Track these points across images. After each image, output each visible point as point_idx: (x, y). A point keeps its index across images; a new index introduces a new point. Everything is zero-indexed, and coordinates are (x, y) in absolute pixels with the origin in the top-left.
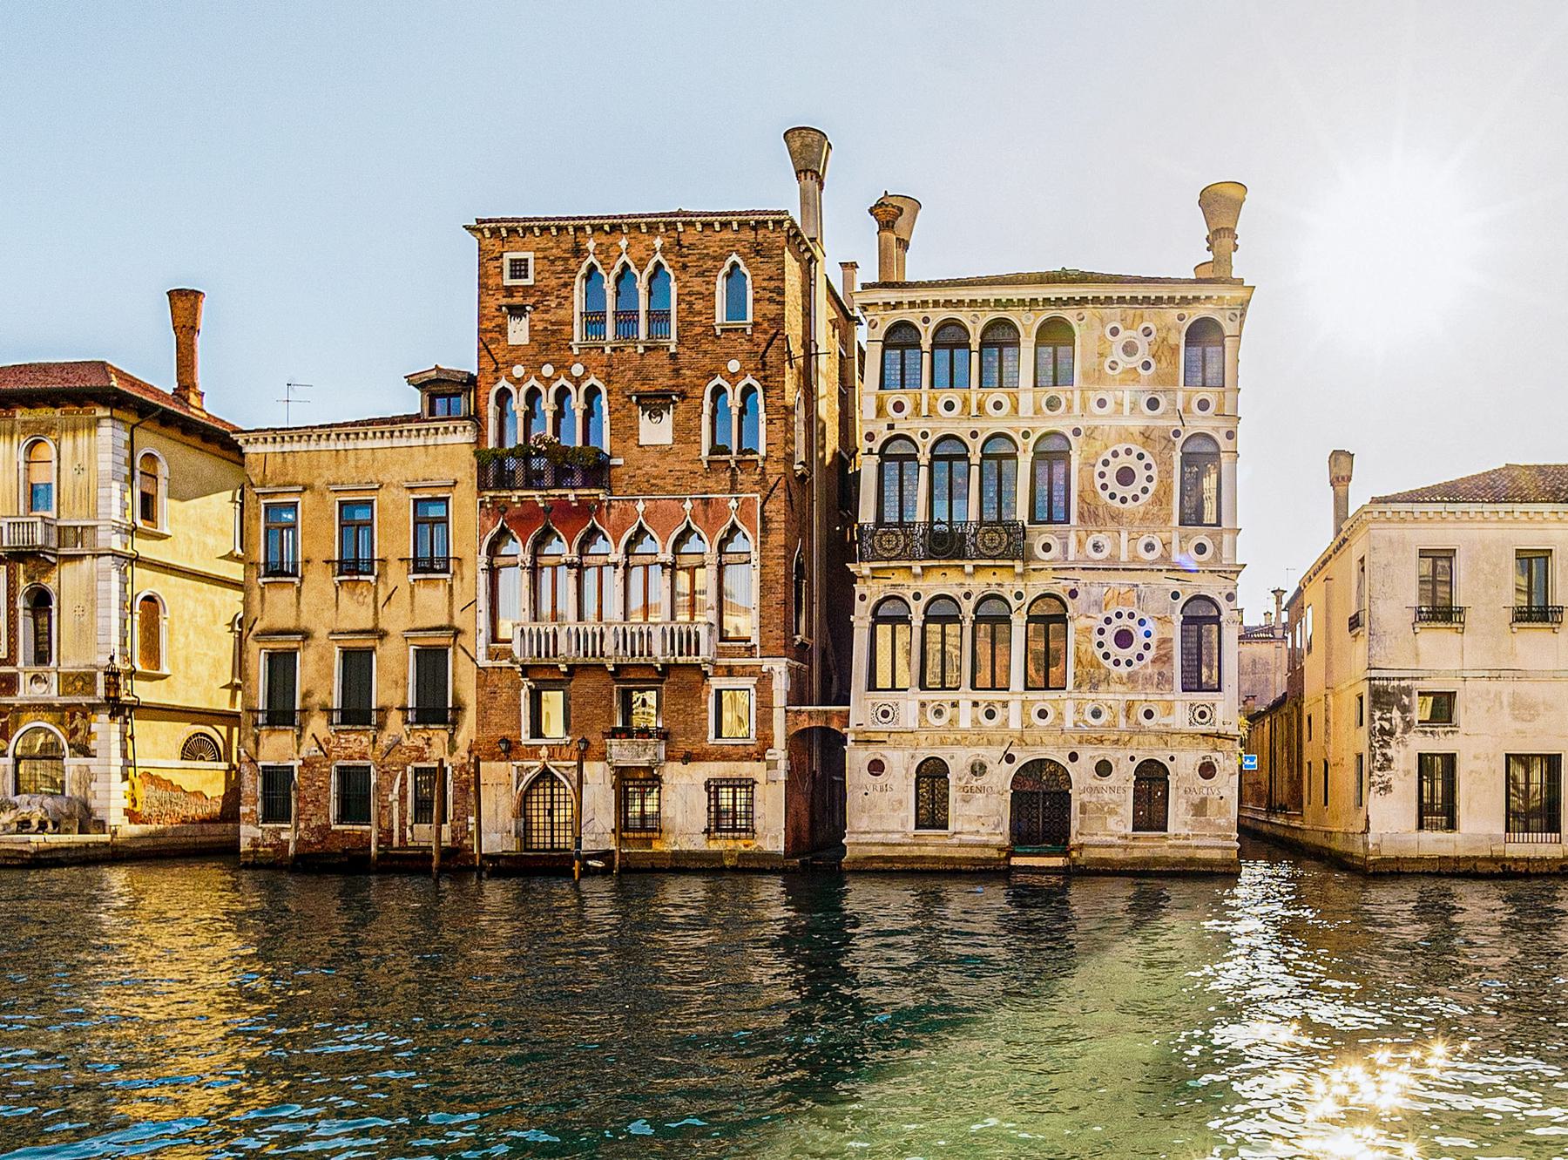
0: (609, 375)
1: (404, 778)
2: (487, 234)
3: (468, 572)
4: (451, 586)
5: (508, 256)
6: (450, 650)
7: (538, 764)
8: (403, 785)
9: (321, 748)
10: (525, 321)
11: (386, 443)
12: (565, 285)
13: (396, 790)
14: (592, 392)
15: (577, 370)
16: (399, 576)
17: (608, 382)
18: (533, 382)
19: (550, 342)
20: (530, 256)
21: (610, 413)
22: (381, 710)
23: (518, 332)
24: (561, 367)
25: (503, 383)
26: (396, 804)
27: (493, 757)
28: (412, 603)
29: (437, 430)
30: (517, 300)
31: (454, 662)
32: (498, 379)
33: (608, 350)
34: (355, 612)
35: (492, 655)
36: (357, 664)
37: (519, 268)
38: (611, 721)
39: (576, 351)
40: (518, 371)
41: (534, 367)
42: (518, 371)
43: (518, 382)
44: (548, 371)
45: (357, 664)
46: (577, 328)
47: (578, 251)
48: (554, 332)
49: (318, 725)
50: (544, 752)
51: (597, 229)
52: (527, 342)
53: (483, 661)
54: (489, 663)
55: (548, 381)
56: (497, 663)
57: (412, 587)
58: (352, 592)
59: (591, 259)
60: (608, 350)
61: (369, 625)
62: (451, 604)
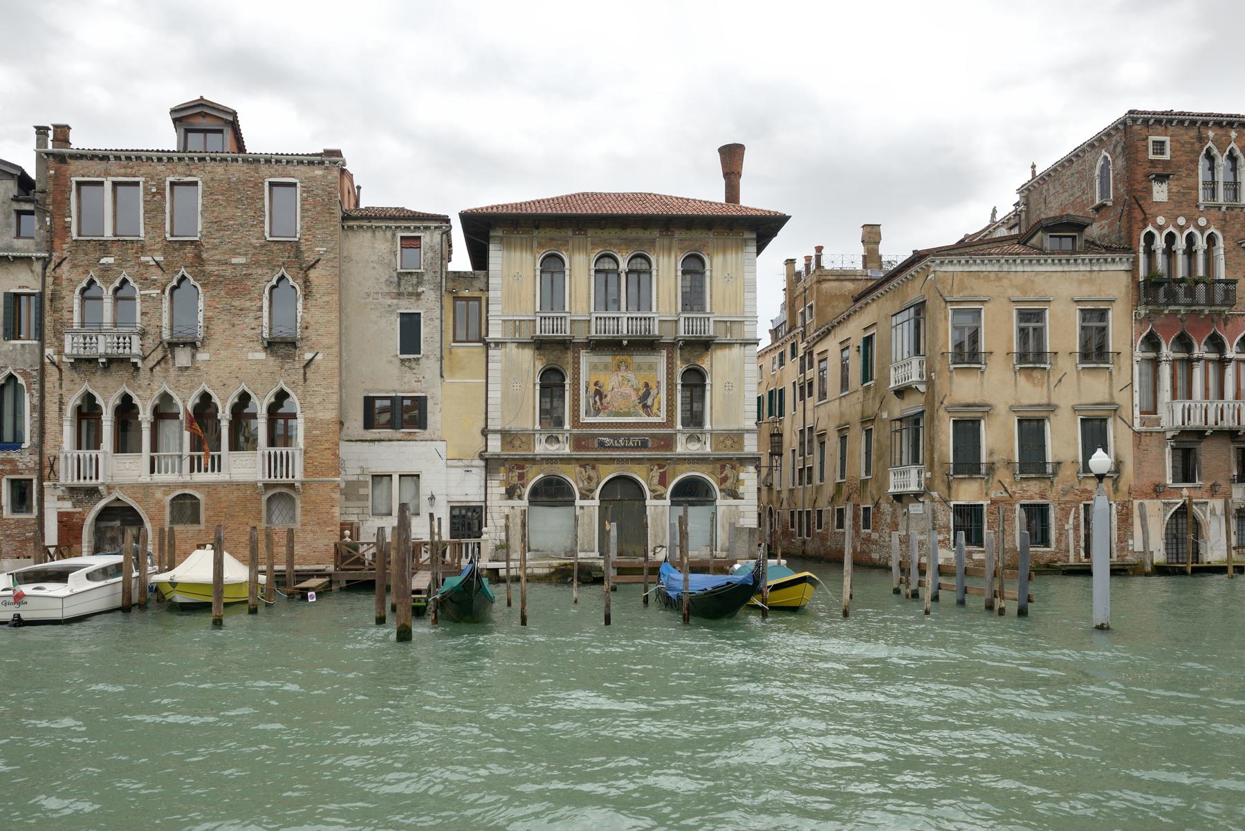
0: (1224, 226)
1: (1077, 512)
2: (1140, 122)
3: (1124, 362)
4: (1111, 373)
5: (1152, 138)
6: (1110, 421)
7: (1181, 501)
8: (1076, 518)
9: (1006, 491)
10: (1165, 186)
11: (1060, 269)
12: (1192, 162)
13: (1071, 521)
14: (1211, 240)
15: (1202, 222)
16: (1068, 365)
17: (1223, 232)
18: (1171, 229)
19: (1184, 201)
20: (1167, 139)
21: (1225, 253)
22: (1059, 463)
23: (1160, 192)
24: (1191, 220)
25: (1150, 228)
26: (1071, 532)
27: (1146, 495)
28: (1079, 385)
29: (1083, 260)
30: (1159, 170)
31: (1115, 428)
32: (1146, 226)
33: (1224, 209)
34: (1031, 393)
35: (1143, 424)
36: (1032, 429)
37: (1159, 147)
38: (1230, 471)
39: (1202, 208)
40: (1161, 220)
41: (1172, 219)
42: (1161, 220)
43: (1160, 228)
44: (1181, 221)
45: (1032, 429)
46: (1201, 192)
47: (1202, 139)
48: (1184, 194)
49: (1003, 475)
50: (1185, 492)
51: (1219, 124)
52: (1166, 200)
53: (1137, 427)
54: (1144, 428)
55: (1181, 229)
56: (1150, 429)
57: (1078, 372)
58: (1029, 377)
59: (1210, 144)
60: (1224, 209)
61: (1045, 401)
62: (1111, 386)
